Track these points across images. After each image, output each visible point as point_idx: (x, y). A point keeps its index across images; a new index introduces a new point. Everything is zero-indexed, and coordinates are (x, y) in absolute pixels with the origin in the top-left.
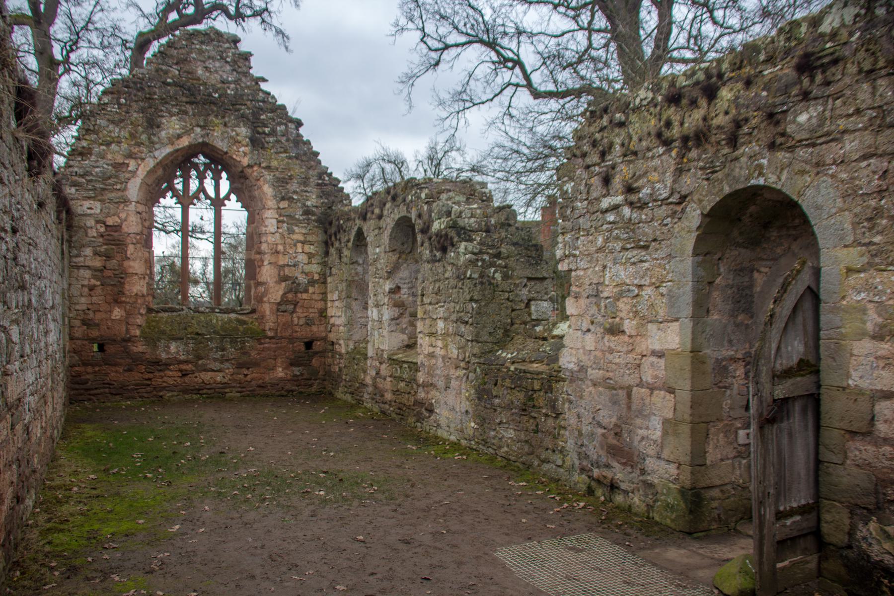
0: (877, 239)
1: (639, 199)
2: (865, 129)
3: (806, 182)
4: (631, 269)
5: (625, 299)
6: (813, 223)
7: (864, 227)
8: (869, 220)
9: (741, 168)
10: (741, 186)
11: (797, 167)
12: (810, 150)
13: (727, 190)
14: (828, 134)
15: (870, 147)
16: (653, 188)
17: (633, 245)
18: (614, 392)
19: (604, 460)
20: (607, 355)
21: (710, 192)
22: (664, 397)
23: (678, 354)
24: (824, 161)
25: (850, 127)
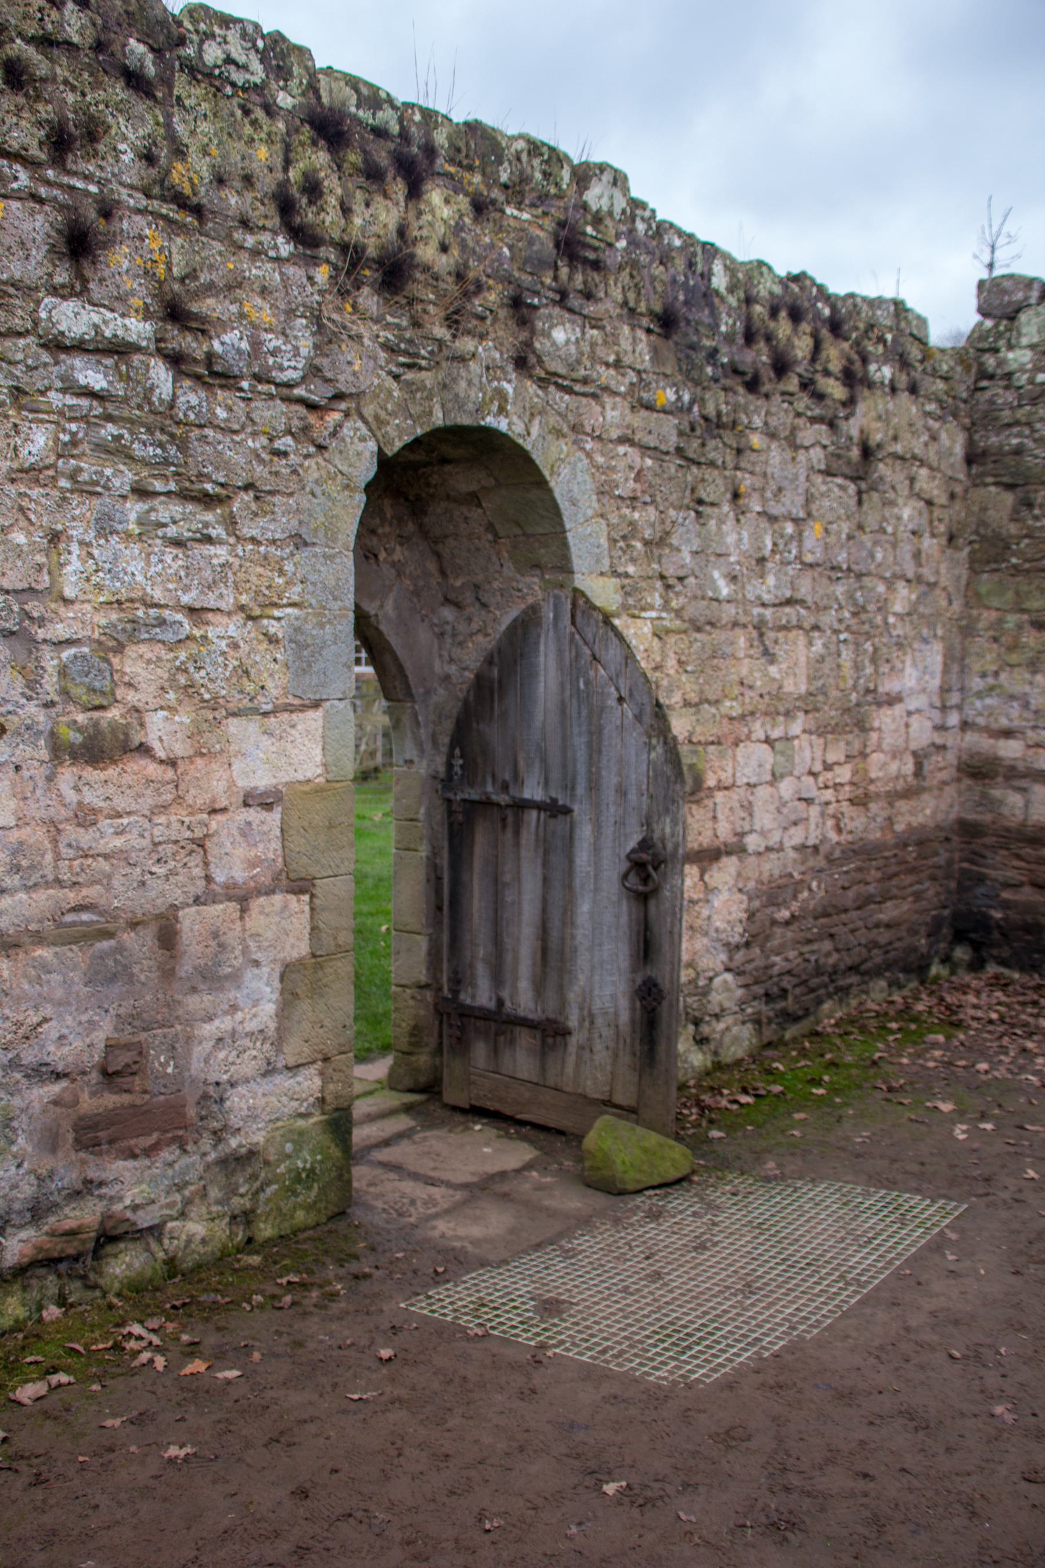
0: (631, 569)
1: (210, 356)
2: (624, 396)
3: (561, 451)
4: (172, 560)
5: (143, 649)
6: (568, 526)
7: (621, 548)
8: (624, 538)
9: (470, 383)
10: (466, 421)
11: (553, 420)
12: (567, 397)
13: (438, 419)
14: (585, 381)
15: (628, 427)
16: (256, 344)
17: (172, 486)
18: (106, 945)
19: (71, 1178)
20: (72, 832)
21: (403, 408)
22: (285, 907)
23: (319, 791)
24: (582, 425)
25: (613, 384)
